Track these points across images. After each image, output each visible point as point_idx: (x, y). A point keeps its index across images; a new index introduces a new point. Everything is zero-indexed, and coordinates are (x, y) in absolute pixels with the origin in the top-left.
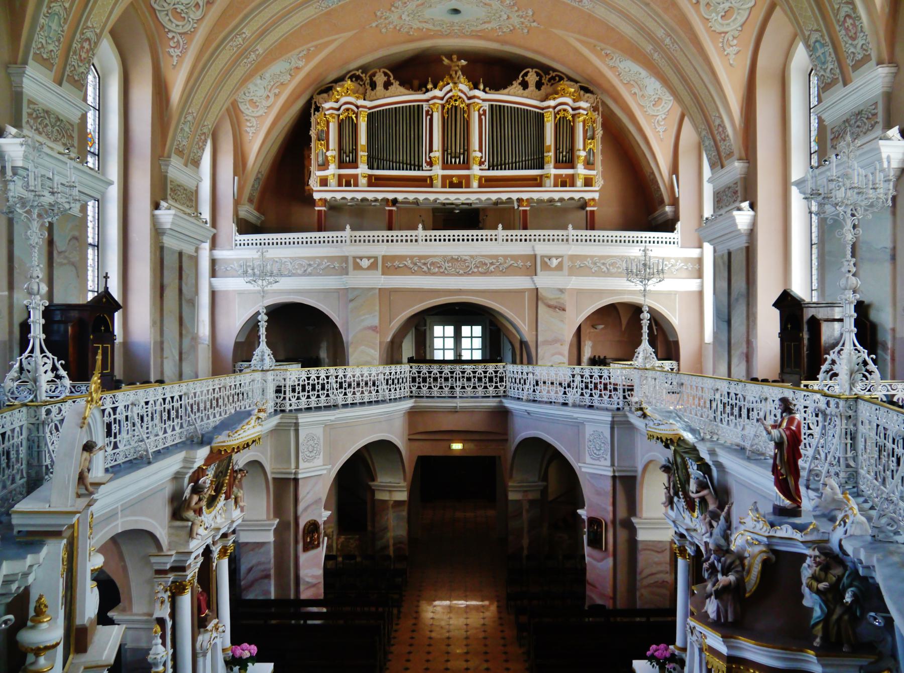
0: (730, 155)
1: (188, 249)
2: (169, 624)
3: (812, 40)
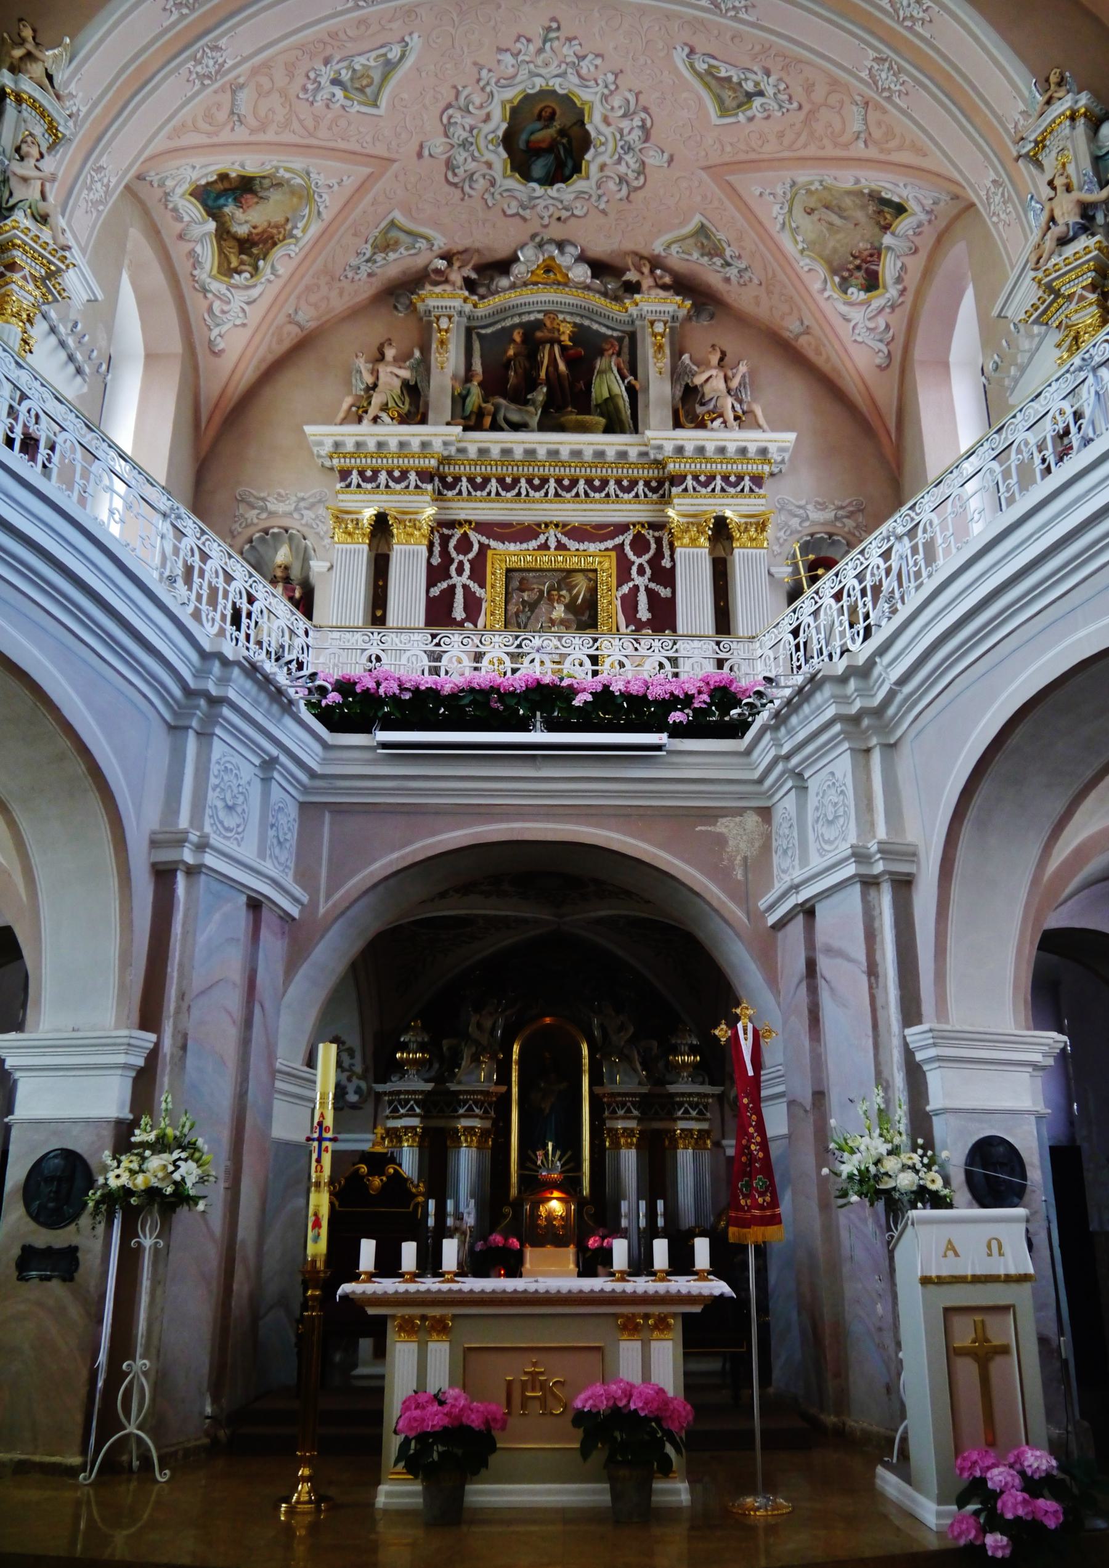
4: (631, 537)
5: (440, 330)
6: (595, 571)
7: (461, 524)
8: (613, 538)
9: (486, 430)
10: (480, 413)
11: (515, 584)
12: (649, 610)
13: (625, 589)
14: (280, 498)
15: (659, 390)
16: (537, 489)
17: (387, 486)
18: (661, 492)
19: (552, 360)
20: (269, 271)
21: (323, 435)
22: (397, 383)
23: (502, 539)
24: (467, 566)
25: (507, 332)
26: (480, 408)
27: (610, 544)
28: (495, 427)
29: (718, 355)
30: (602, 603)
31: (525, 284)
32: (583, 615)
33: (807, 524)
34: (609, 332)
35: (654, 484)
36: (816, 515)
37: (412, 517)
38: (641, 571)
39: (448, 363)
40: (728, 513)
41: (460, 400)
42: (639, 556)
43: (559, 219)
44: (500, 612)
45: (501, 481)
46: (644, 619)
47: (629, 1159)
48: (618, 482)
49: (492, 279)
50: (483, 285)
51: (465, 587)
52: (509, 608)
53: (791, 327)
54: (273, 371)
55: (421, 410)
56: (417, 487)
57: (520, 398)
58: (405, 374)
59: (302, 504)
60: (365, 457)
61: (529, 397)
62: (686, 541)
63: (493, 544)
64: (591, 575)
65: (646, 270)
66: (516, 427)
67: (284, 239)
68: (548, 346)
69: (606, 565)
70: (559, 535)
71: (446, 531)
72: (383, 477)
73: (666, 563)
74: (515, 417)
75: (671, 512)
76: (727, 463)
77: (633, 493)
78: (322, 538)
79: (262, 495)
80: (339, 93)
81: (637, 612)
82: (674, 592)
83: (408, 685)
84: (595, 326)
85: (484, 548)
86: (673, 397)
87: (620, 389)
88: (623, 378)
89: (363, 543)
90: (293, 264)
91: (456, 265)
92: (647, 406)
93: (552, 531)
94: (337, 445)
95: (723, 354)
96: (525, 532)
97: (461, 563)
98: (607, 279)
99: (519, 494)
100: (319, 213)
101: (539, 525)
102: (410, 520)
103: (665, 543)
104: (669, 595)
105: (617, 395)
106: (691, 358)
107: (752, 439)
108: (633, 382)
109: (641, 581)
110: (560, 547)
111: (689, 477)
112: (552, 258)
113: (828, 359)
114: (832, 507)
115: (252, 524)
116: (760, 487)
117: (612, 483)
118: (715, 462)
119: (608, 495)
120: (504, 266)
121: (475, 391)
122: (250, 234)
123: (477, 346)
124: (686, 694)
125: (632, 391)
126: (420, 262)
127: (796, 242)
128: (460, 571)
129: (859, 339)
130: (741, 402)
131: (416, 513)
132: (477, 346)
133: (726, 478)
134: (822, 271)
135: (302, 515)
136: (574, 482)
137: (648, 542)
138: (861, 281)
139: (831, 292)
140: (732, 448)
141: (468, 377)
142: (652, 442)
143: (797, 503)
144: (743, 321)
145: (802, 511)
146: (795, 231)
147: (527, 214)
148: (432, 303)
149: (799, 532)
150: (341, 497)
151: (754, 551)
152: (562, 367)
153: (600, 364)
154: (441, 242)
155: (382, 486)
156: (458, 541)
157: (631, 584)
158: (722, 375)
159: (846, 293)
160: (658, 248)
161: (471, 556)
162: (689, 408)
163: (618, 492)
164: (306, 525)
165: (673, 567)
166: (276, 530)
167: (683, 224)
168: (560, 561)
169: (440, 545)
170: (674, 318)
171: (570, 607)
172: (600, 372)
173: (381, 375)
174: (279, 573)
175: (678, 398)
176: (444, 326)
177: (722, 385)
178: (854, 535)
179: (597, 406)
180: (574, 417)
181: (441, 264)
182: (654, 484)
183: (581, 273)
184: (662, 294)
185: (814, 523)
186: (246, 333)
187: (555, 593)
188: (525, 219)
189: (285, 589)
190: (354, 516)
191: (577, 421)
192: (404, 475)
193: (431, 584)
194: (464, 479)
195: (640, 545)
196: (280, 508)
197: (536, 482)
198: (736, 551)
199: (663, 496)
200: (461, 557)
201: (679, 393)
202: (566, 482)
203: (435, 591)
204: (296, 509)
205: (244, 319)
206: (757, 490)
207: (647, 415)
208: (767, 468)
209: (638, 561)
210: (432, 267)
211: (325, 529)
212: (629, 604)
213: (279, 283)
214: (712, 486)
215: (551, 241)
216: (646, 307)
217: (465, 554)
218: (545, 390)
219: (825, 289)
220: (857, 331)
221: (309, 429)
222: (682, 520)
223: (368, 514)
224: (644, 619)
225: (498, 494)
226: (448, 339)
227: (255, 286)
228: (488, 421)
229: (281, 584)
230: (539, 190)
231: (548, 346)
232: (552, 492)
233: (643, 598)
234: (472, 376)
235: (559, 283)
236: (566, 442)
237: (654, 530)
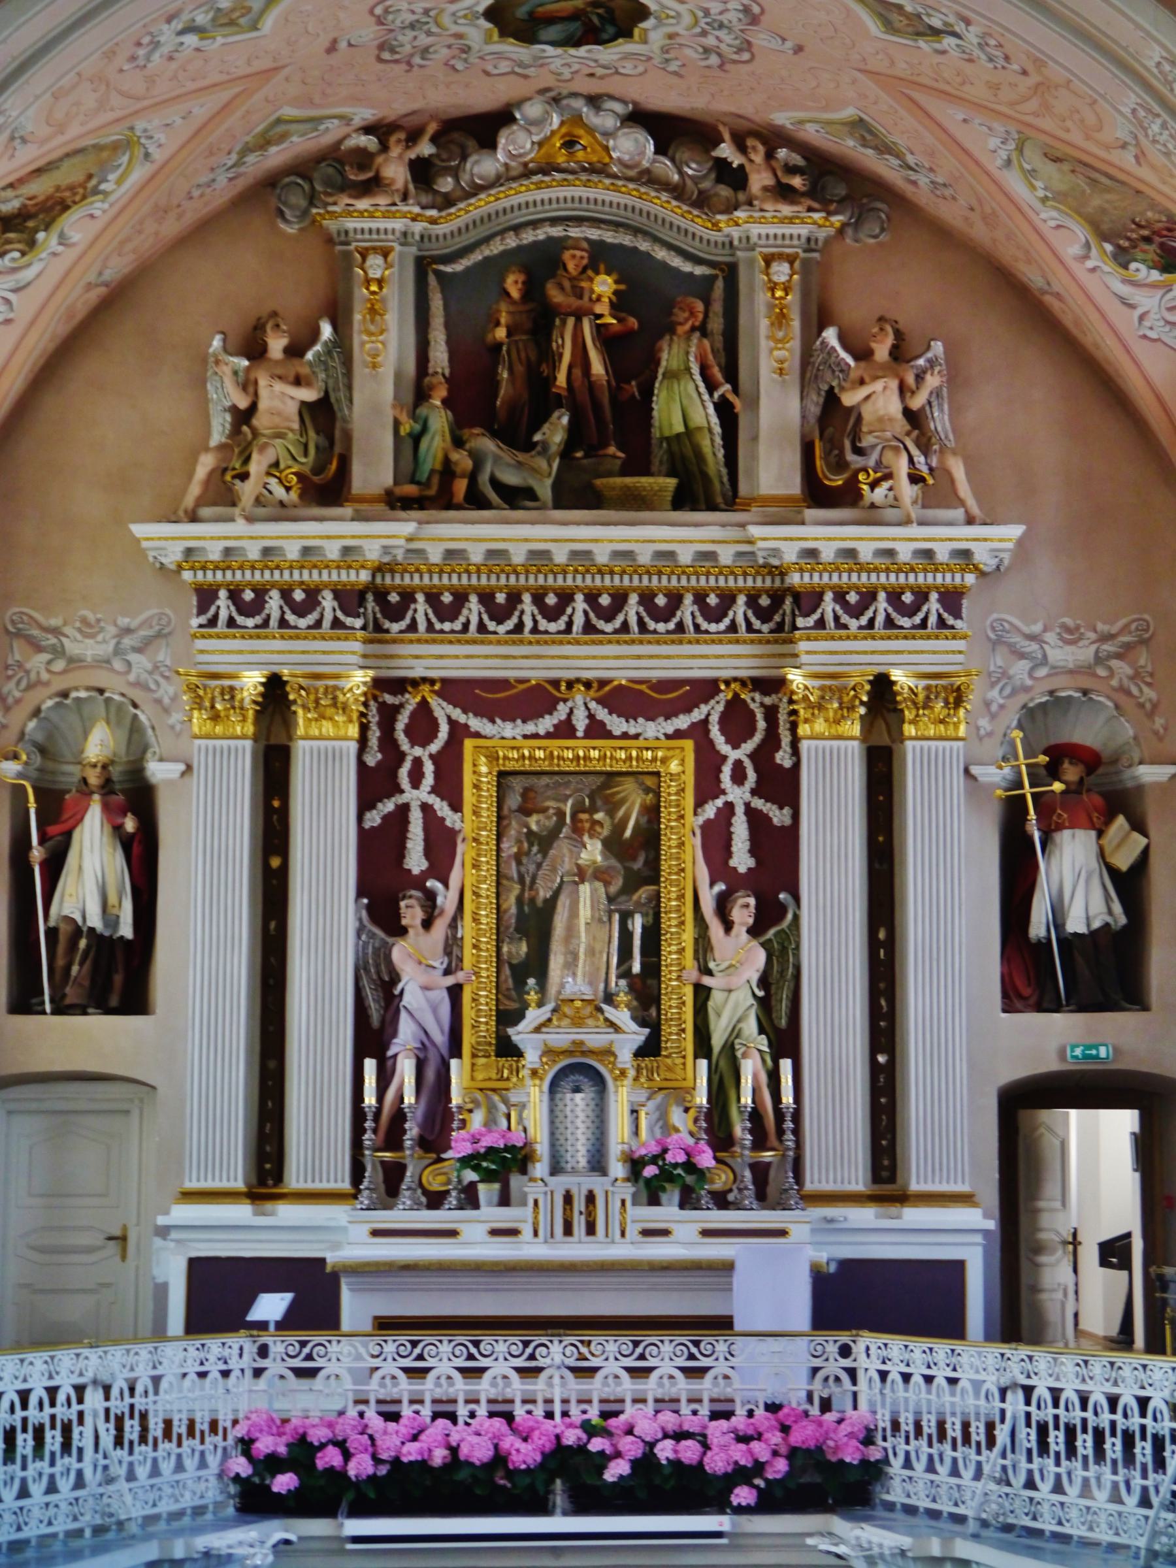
4: (720, 708)
5: (368, 282)
6: (658, 774)
7: (415, 683)
8: (689, 710)
9: (459, 507)
10: (447, 471)
11: (513, 801)
12: (753, 852)
13: (710, 811)
14: (88, 629)
15: (778, 412)
16: (552, 614)
17: (283, 624)
18: (777, 618)
19: (580, 353)
20: (54, 240)
21: (164, 539)
22: (292, 409)
23: (490, 712)
24: (429, 768)
25: (496, 267)
26: (447, 461)
27: (682, 722)
28: (476, 501)
29: (890, 340)
30: (668, 842)
31: (527, 173)
32: (634, 859)
33: (1042, 672)
34: (687, 267)
35: (764, 601)
36: (1061, 655)
37: (331, 683)
38: (739, 776)
39: (386, 348)
40: (897, 675)
41: (409, 444)
42: (736, 746)
43: (592, 75)
44: (488, 861)
45: (486, 598)
46: (742, 869)
48: (700, 598)
49: (464, 158)
50: (448, 171)
51: (426, 808)
52: (504, 846)
53: (1033, 277)
55: (338, 449)
56: (337, 624)
57: (517, 435)
58: (309, 395)
59: (127, 642)
60: (241, 568)
61: (537, 437)
62: (820, 726)
63: (475, 723)
64: (650, 782)
65: (758, 157)
66: (516, 498)
67: (84, 197)
68: (571, 321)
69: (674, 767)
70: (593, 705)
71: (389, 699)
72: (274, 602)
73: (783, 758)
74: (511, 478)
75: (796, 678)
76: (900, 570)
77: (726, 621)
78: (167, 711)
79: (54, 622)
80: (191, 40)
81: (729, 854)
82: (796, 816)
83: (384, 1456)
84: (661, 254)
85: (458, 732)
86: (804, 417)
87: (705, 415)
88: (711, 387)
89: (243, 737)
90: (97, 225)
91: (395, 151)
92: (755, 438)
93: (579, 697)
94: (189, 552)
95: (898, 334)
96: (532, 700)
97: (418, 762)
98: (683, 154)
99: (519, 628)
100: (147, 155)
101: (555, 683)
102: (329, 699)
103: (782, 717)
104: (788, 821)
105: (699, 429)
106: (842, 338)
107: (946, 537)
108: (731, 397)
109: (737, 795)
110: (597, 730)
111: (829, 596)
112: (578, 119)
113: (1098, 348)
114: (1092, 636)
115: (39, 683)
116: (958, 615)
117: (688, 599)
118: (876, 570)
119: (680, 627)
120: (485, 128)
121: (439, 420)
122: (24, 206)
123: (437, 303)
124: (756, 1461)
125: (725, 410)
126: (327, 140)
127: (1033, 188)
128: (416, 778)
129: (1153, 335)
130: (926, 450)
131: (337, 677)
132: (437, 303)
133: (894, 597)
134: (1082, 232)
135: (129, 664)
136: (620, 599)
137: (752, 714)
138: (1151, 256)
139: (1100, 257)
140: (905, 553)
141: (421, 394)
142: (761, 544)
143: (1026, 630)
144: (943, 235)
145: (1034, 647)
146: (1030, 175)
147: (531, 71)
148: (351, 224)
149: (1026, 689)
150: (200, 644)
151: (940, 744)
152: (598, 368)
153: (670, 356)
154: (364, 115)
155: (274, 622)
156: (413, 715)
157: (719, 802)
158: (894, 384)
159: (1125, 267)
160: (782, 118)
161: (434, 747)
163: (700, 620)
164: (137, 684)
165: (797, 766)
166: (83, 694)
167: (825, 109)
168: (594, 753)
169: (379, 724)
170: (810, 244)
171: (613, 845)
172: (671, 375)
173: (263, 392)
174: (94, 779)
175: (812, 420)
176: (375, 273)
177: (894, 407)
178: (1128, 693)
179: (663, 439)
180: (619, 481)
181: (369, 142)
182: (764, 601)
183: (633, 146)
184: (787, 210)
185: (1056, 671)
186: (15, 331)
187: (584, 816)
188: (526, 77)
189: (106, 807)
190: (227, 683)
191: (627, 488)
192: (313, 595)
193: (365, 803)
194: (420, 598)
195: (737, 722)
196: (89, 649)
197: (551, 600)
198: (909, 744)
199: (780, 628)
200: (418, 751)
201: (815, 410)
202: (605, 600)
203: (374, 819)
204: (117, 651)
206: (950, 621)
207: (754, 457)
208: (970, 579)
209: (733, 755)
210: (352, 142)
211: (171, 690)
212: (716, 839)
213: (71, 255)
214: (869, 614)
215: (574, 95)
216: (755, 230)
217: (424, 745)
218: (565, 420)
219: (1086, 257)
220: (1147, 323)
221: (139, 530)
222: (810, 683)
223: (251, 681)
224: (742, 869)
225: (482, 628)
226: (383, 301)
227: (29, 265)
228: (461, 487)
229: (96, 797)
230: (550, 50)
231: (571, 321)
232: (579, 621)
233: (740, 829)
234: (431, 388)
235: (593, 170)
237: (766, 693)
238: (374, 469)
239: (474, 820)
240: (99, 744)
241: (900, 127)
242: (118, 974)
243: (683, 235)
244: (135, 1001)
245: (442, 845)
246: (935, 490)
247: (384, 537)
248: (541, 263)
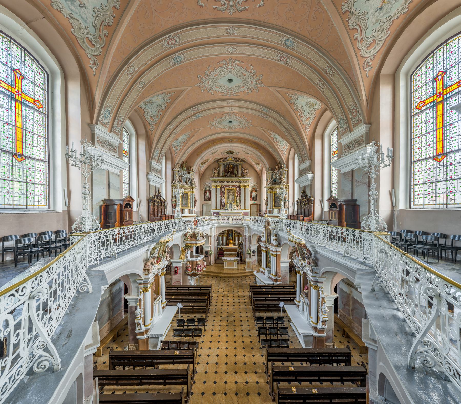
0: (306, 159)
1: (158, 186)
2: (142, 300)
3: (340, 119)
15: (240, 172)
39: (221, 169)
47: (236, 238)
54: (205, 170)
57: (228, 173)
96: (229, 186)
102: (219, 186)
107: (248, 178)
120: (226, 158)
144: (248, 163)
162: (243, 175)
183: (233, 159)
205: (203, 168)
236: (232, 178)
238: (221, 175)
239: (226, 192)
240: (208, 188)
241: (246, 158)
242: (209, 199)
243: (236, 163)
244: (210, 200)
245: (224, 193)
246: (247, 176)
247: (221, 178)
248: (229, 165)
